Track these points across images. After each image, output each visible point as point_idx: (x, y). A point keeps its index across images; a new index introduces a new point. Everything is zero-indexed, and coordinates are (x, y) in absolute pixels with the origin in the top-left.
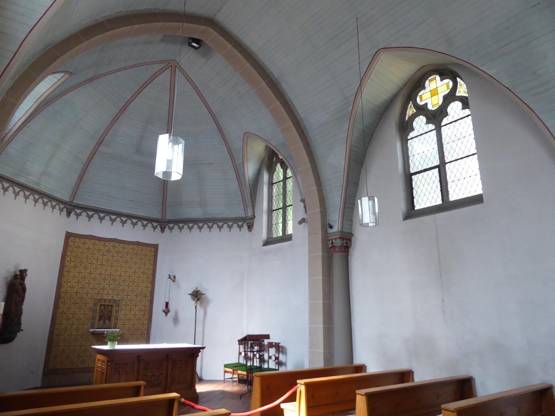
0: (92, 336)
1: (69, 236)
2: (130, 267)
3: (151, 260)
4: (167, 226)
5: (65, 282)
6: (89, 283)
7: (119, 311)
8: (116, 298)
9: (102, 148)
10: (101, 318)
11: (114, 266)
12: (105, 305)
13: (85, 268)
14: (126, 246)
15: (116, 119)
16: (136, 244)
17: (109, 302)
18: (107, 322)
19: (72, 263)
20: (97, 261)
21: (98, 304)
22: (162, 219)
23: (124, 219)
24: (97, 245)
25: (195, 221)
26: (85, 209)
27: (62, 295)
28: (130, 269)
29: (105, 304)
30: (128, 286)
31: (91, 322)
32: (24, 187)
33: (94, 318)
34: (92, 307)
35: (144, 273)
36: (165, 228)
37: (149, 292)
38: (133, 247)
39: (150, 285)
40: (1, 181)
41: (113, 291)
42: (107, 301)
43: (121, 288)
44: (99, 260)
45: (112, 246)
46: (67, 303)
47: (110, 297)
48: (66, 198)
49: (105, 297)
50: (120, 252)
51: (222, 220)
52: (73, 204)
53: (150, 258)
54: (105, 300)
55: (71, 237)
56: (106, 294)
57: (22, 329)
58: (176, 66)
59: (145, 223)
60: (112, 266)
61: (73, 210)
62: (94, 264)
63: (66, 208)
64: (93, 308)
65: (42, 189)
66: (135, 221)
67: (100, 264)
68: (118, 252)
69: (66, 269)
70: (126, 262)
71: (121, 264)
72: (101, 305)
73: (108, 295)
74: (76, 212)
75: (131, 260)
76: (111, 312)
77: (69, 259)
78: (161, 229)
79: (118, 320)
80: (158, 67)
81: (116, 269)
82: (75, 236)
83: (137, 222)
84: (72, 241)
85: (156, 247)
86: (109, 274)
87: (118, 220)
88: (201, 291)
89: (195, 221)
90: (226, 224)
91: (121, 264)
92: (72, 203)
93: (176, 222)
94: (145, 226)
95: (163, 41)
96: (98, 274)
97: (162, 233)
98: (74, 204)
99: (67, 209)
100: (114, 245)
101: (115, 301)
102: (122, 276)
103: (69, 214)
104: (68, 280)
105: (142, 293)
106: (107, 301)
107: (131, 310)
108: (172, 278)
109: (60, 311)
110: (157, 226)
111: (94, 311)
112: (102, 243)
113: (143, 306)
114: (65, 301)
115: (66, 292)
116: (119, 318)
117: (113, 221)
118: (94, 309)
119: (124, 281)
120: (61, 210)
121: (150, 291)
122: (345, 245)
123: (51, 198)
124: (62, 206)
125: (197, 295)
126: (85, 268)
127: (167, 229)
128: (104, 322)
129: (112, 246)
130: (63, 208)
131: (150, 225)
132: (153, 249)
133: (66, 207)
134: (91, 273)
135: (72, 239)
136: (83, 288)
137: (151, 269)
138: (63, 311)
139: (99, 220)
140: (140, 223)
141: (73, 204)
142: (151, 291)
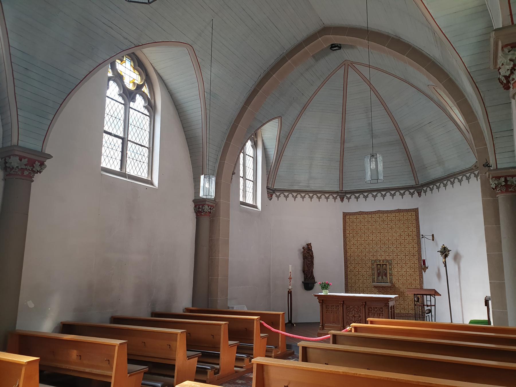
0: (374, 288)
1: (345, 215)
2: (396, 232)
3: (414, 223)
4: (422, 190)
5: (349, 249)
6: (365, 248)
7: (392, 269)
8: (387, 258)
9: (346, 145)
10: (379, 274)
11: (382, 233)
12: (381, 264)
13: (361, 237)
14: (389, 215)
15: (344, 120)
16: (397, 211)
17: (383, 262)
18: (384, 277)
19: (351, 235)
20: (368, 230)
21: (375, 264)
22: (416, 185)
23: (384, 193)
24: (366, 218)
25: (440, 180)
26: (353, 193)
27: (349, 258)
28: (396, 234)
29: (380, 263)
30: (397, 248)
31: (372, 277)
32: (299, 192)
33: (373, 275)
34: (371, 266)
35: (409, 235)
36: (421, 192)
37: (416, 251)
38: (395, 215)
39: (416, 245)
40: (283, 193)
41: (385, 253)
42: (381, 262)
43: (391, 250)
44: (370, 229)
45: (378, 217)
46: (353, 264)
47: (383, 258)
48: (338, 189)
49: (379, 258)
50: (385, 221)
51: (469, 170)
52: (342, 192)
53: (412, 222)
54: (380, 261)
55: (347, 216)
56: (379, 256)
57: (316, 281)
58: (351, 63)
59: (402, 192)
60: (380, 233)
61: (345, 195)
62: (366, 233)
63: (339, 196)
64: (372, 267)
65: (313, 189)
66: (393, 192)
67: (371, 233)
68: (383, 221)
69: (348, 239)
70: (392, 228)
71: (388, 231)
72: (377, 264)
73: (382, 257)
74: (347, 197)
75: (396, 226)
76: (386, 270)
77: (348, 232)
78: (418, 194)
79: (392, 275)
80: (341, 71)
81: (384, 235)
82: (349, 215)
83: (395, 193)
84: (348, 219)
85: (416, 211)
86: (379, 239)
87: (379, 195)
88: (447, 247)
89: (440, 180)
90: (464, 177)
91: (388, 231)
92: (342, 191)
93: (427, 184)
94: (402, 195)
95: (317, 60)
96: (371, 240)
97: (420, 197)
98: (343, 191)
99: (340, 196)
100: (379, 215)
101: (387, 261)
102: (390, 240)
103: (342, 200)
104: (350, 247)
105: (409, 253)
106: (381, 262)
107: (402, 268)
108: (431, 238)
109: (349, 269)
110: (414, 192)
111: (373, 269)
112: (370, 216)
113: (412, 264)
114: (351, 262)
115: (350, 256)
116: (393, 274)
117: (375, 197)
118: (372, 268)
119: (393, 244)
120: (335, 198)
121: (417, 250)
122: (503, 184)
123: (323, 192)
124: (335, 196)
125: (445, 252)
126: (361, 237)
127: (423, 193)
128: (382, 278)
129: (378, 217)
130: (336, 197)
131: (407, 193)
132: (414, 213)
133: (339, 195)
134: (365, 241)
135: (347, 217)
136: (362, 252)
137: (414, 231)
138: (351, 270)
139: (364, 199)
140: (398, 193)
141: (342, 192)
142: (418, 250)
